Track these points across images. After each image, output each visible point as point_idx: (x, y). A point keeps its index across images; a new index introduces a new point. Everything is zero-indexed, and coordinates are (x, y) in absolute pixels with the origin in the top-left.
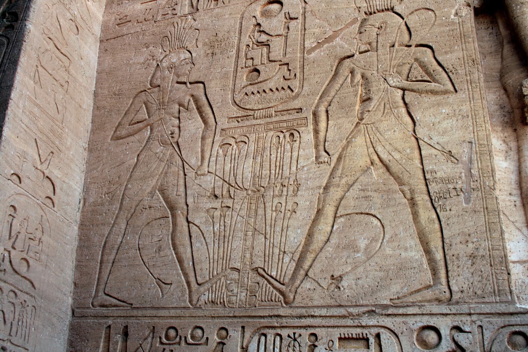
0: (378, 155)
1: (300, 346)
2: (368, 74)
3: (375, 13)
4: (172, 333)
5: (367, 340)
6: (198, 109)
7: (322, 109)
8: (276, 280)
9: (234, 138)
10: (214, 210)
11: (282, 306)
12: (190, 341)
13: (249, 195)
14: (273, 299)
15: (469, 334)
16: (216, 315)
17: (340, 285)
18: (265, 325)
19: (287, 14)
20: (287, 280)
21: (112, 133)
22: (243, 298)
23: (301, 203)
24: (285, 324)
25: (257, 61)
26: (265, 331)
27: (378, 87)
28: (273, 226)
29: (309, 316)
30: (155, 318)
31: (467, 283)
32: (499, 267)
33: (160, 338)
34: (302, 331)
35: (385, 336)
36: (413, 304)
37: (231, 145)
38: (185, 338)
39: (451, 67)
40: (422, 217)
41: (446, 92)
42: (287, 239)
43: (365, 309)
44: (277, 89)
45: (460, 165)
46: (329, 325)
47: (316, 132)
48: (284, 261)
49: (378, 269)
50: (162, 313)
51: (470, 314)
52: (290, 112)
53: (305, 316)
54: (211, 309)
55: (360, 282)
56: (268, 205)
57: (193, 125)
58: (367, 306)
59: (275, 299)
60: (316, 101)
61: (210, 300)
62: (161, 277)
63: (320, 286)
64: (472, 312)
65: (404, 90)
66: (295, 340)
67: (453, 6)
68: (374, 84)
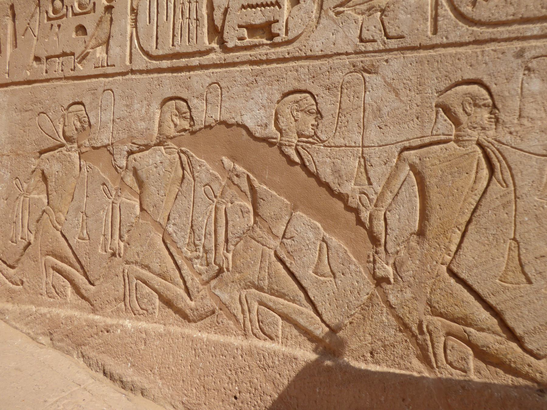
12: (77, 10)
38: (72, 7)
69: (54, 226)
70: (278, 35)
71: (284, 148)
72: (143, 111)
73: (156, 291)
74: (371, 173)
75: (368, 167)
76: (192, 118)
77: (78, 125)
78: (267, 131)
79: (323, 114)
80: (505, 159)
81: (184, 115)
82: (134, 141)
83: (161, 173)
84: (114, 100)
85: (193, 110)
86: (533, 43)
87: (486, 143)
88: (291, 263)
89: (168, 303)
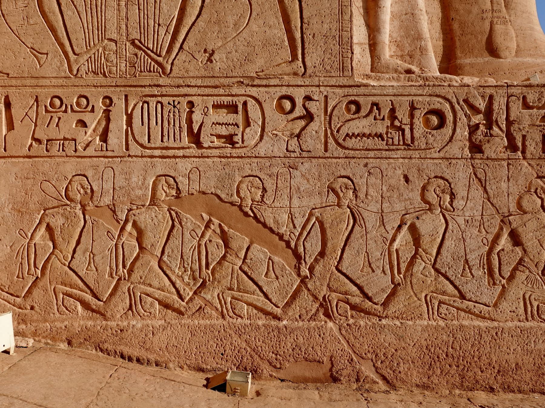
1: (179, 112)
4: (57, 102)
5: (236, 106)
8: (152, 51)
11: (161, 76)
14: (152, 69)
16: (98, 85)
17: (212, 58)
20: (164, 53)
22: (124, 69)
24: (165, 93)
29: (185, 86)
30: (37, 87)
31: (319, 59)
32: (346, 47)
33: (46, 106)
34: (181, 99)
35: (251, 103)
36: (275, 77)
42: (161, 11)
43: (235, 80)
46: (204, 94)
48: (160, 33)
49: (246, 44)
51: (319, 86)
53: (182, 86)
54: (92, 78)
55: (230, 55)
58: (237, 77)
59: (154, 70)
61: (91, 70)
62: (35, 47)
64: (321, 84)
66: (174, 107)
69: (62, 263)
70: (237, 143)
71: (243, 208)
72: (140, 183)
73: (157, 300)
74: (295, 222)
75: (294, 218)
76: (178, 188)
77: (82, 191)
78: (232, 198)
79: (267, 189)
80: (361, 214)
81: (172, 186)
82: (133, 203)
83: (156, 223)
84: (114, 174)
85: (179, 184)
86: (371, 160)
87: (352, 207)
88: (251, 273)
89: (166, 306)
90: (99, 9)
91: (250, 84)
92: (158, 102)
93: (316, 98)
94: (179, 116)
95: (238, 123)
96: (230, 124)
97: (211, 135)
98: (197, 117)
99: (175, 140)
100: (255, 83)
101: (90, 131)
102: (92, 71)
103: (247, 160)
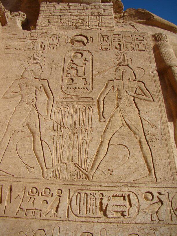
0: (125, 122)
2: (120, 88)
3: (121, 65)
4: (35, 190)
6: (45, 91)
7: (101, 100)
8: (84, 169)
9: (62, 106)
10: (54, 136)
13: (70, 131)
14: (83, 177)
15: (164, 196)
17: (112, 174)
18: (80, 189)
19: (85, 58)
20: (89, 170)
21: (3, 95)
23: (94, 137)
24: (89, 189)
25: (72, 75)
26: (80, 191)
27: (124, 94)
28: (82, 146)
33: (29, 192)
34: (97, 192)
36: (143, 183)
37: (61, 109)
38: (41, 193)
39: (152, 92)
40: (144, 148)
41: (150, 101)
43: (123, 184)
44: (81, 88)
45: (157, 129)
47: (99, 108)
49: (128, 168)
50: (29, 180)
52: (87, 98)
55: (121, 172)
56: (79, 136)
57: (42, 98)
58: (124, 183)
59: (84, 178)
60: (99, 96)
61: (53, 176)
62: (28, 164)
63: (104, 173)
65: (134, 97)
66: (93, 196)
67: (151, 69)
68: (122, 93)
70: (126, 215)
90: (60, 150)
91: (131, 186)
92: (86, 193)
93: (163, 193)
94: (96, 201)
95: (125, 205)
96: (121, 206)
97: (112, 211)
98: (105, 202)
99: (93, 213)
100: (133, 186)
101: (49, 206)
102: (54, 177)
103: (131, 225)
